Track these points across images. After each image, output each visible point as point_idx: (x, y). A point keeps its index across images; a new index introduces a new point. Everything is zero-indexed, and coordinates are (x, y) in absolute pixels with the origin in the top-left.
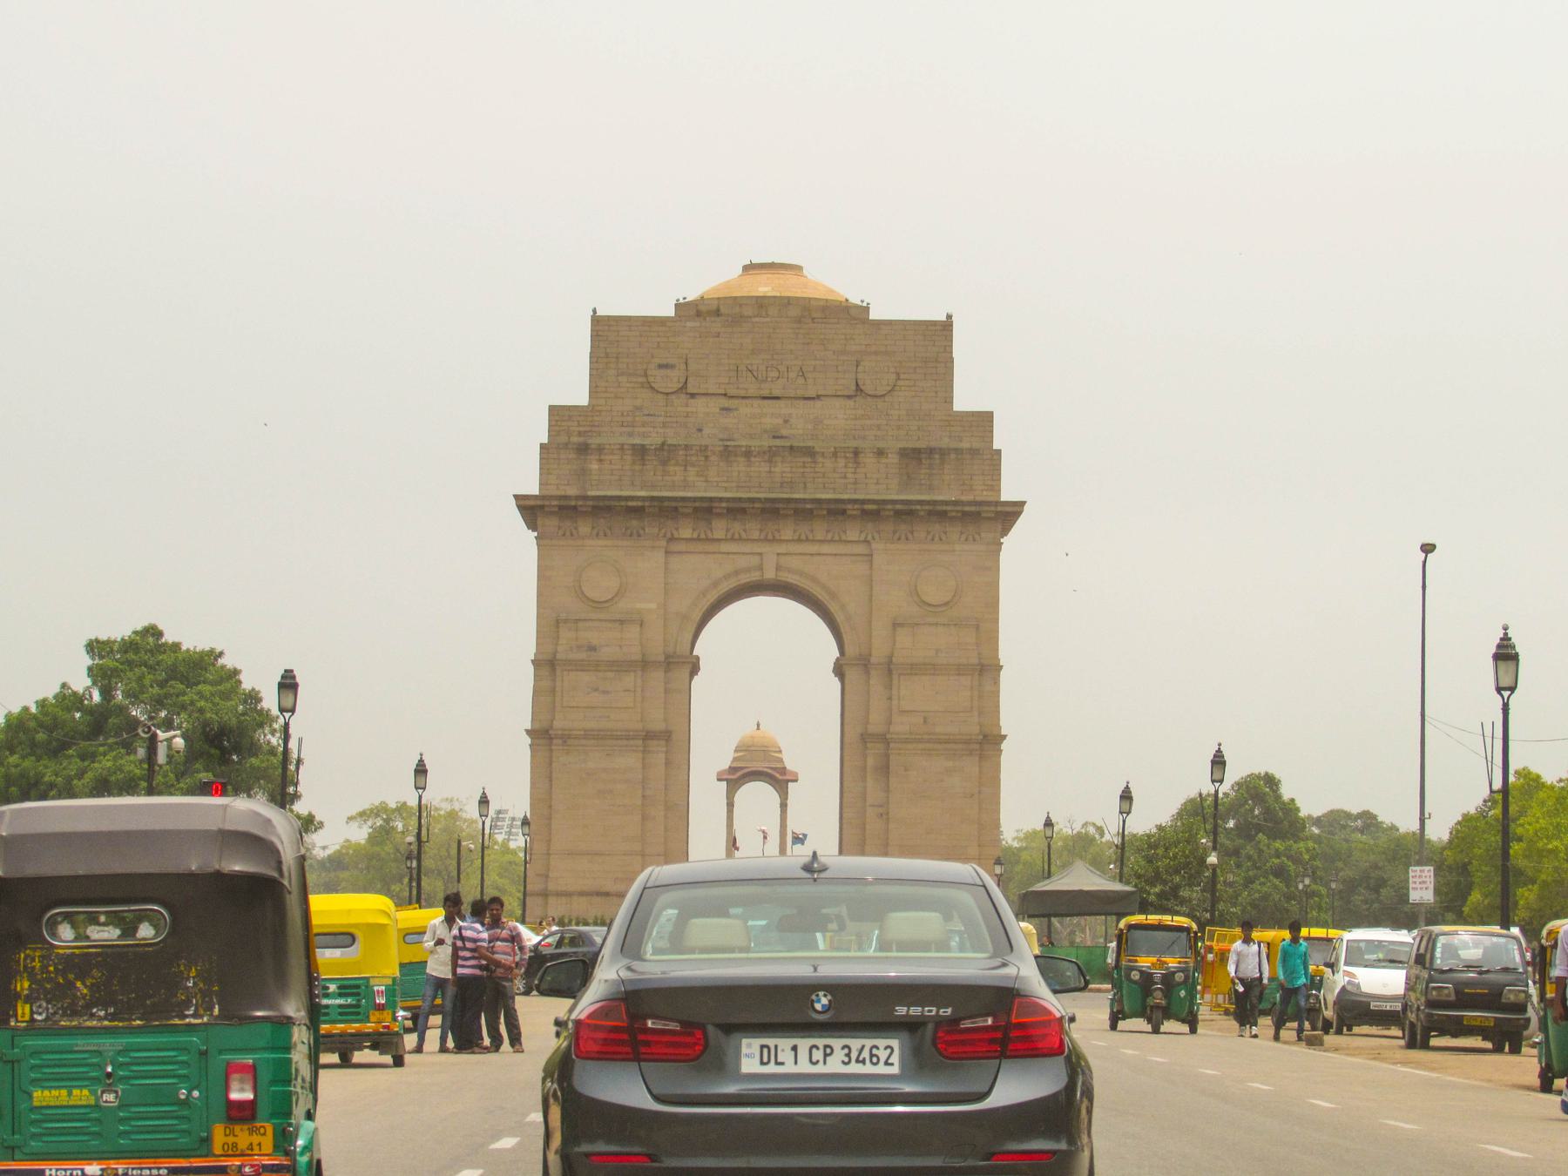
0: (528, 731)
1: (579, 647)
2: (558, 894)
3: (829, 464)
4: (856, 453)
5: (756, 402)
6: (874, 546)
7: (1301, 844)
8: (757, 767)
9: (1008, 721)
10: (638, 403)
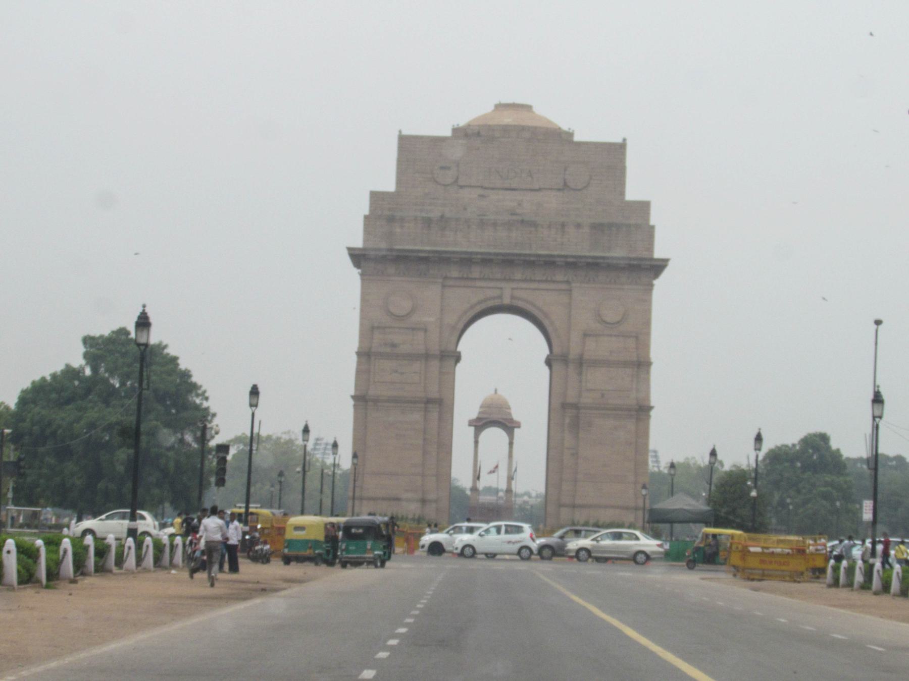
2: (370, 499)
4: (563, 225)
5: (501, 192)
6: (573, 285)
7: (841, 478)
8: (495, 417)
9: (655, 399)
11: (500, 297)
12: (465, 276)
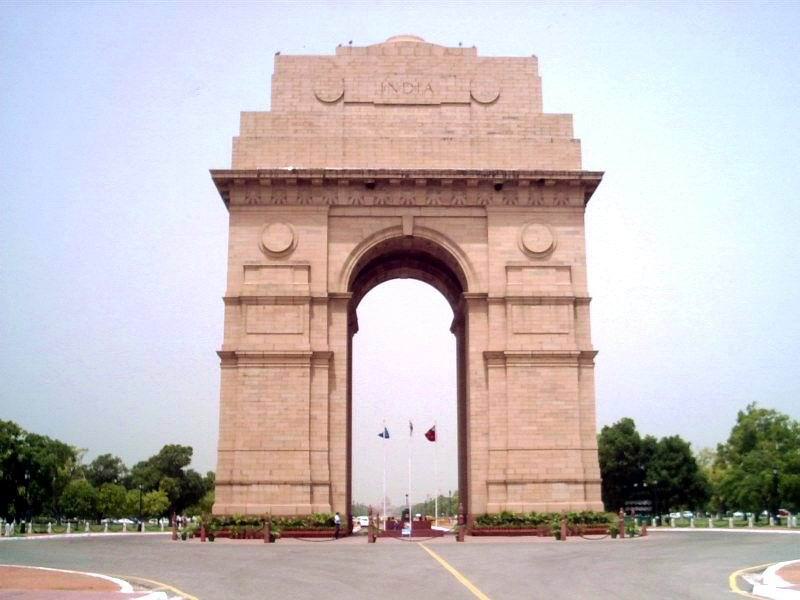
0: (218, 353)
6: (488, 209)
11: (400, 227)
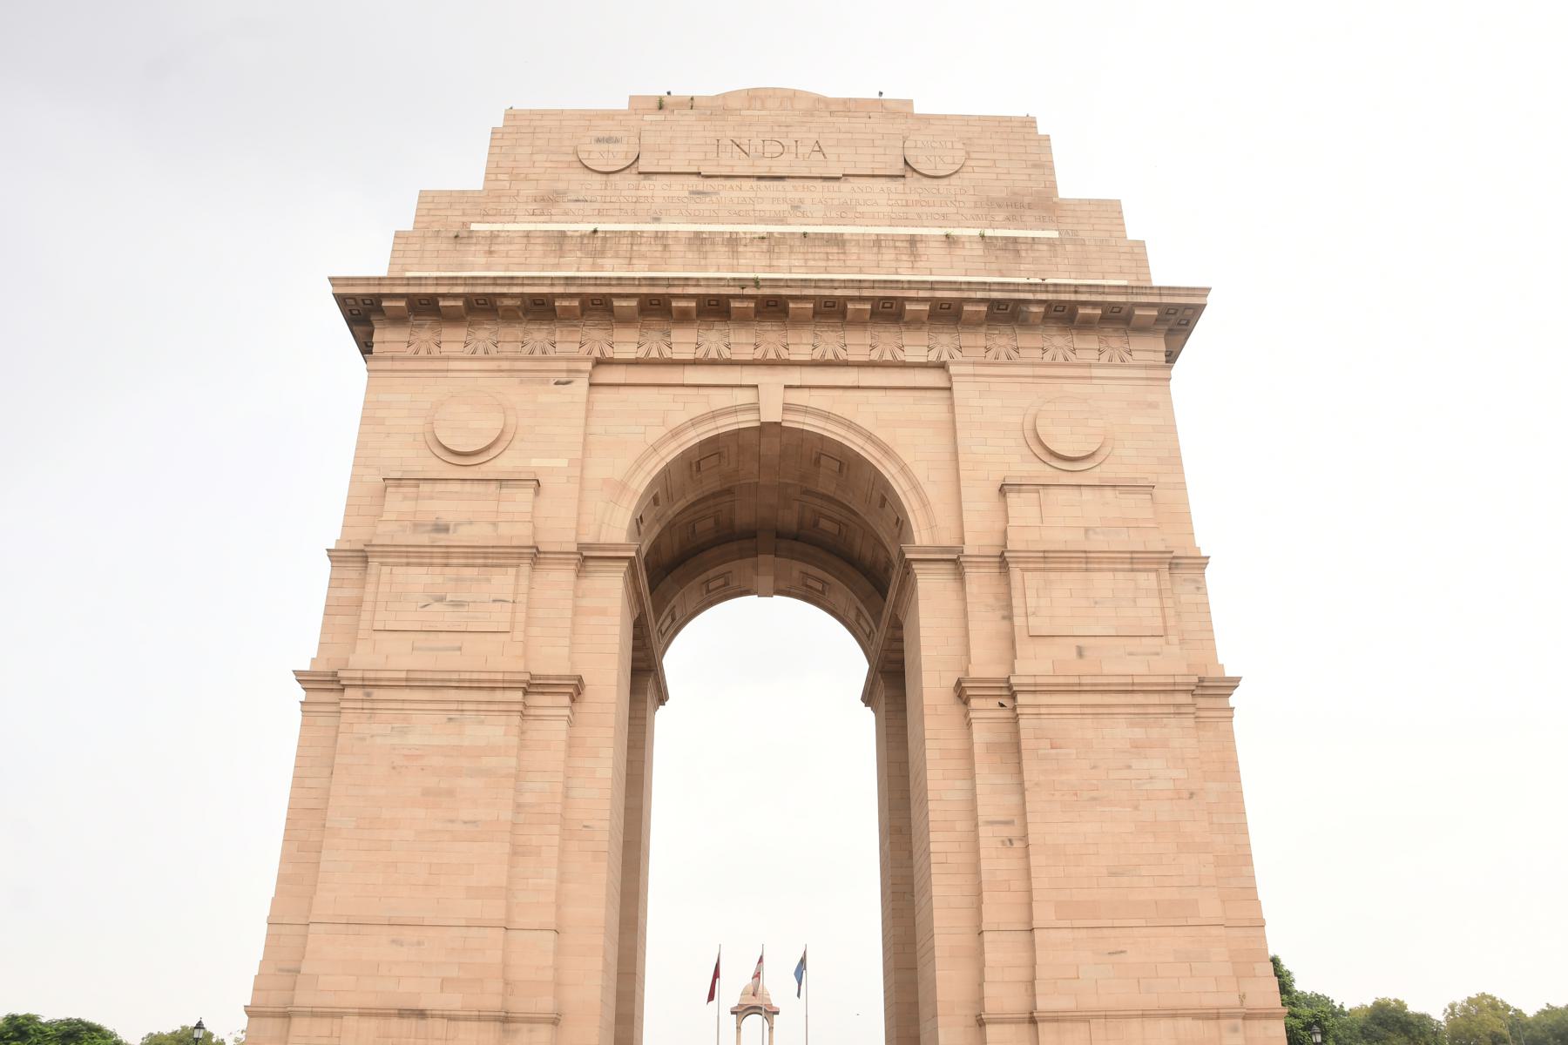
1: (417, 526)
2: (314, 1014)
3: (869, 257)
6: (953, 369)
10: (561, 186)
11: (756, 408)
12: (654, 354)
